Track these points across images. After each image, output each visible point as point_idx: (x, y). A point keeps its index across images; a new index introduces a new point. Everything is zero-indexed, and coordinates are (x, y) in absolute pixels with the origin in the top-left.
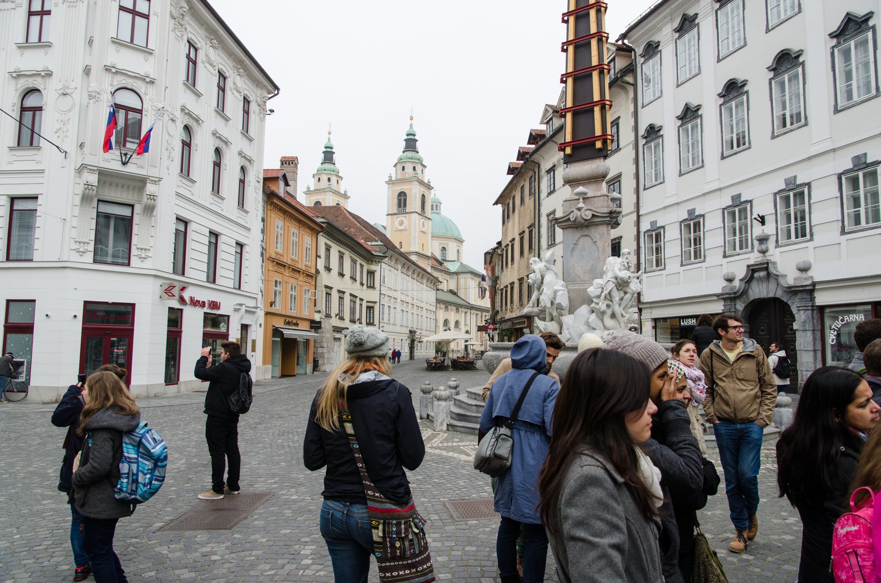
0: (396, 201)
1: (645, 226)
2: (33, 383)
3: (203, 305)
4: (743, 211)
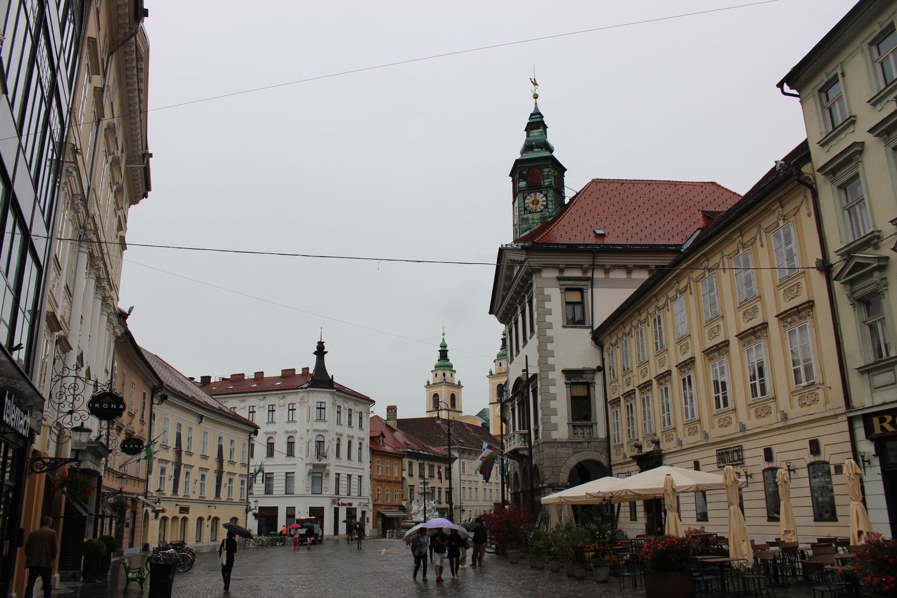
0: (496, 392)
3: (345, 505)
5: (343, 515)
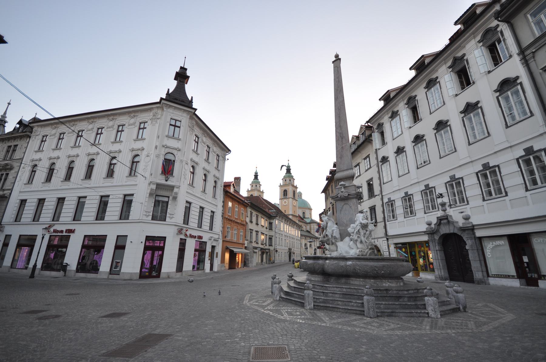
1: (386, 200)
2: (122, 271)
4: (431, 192)
5: (191, 246)
